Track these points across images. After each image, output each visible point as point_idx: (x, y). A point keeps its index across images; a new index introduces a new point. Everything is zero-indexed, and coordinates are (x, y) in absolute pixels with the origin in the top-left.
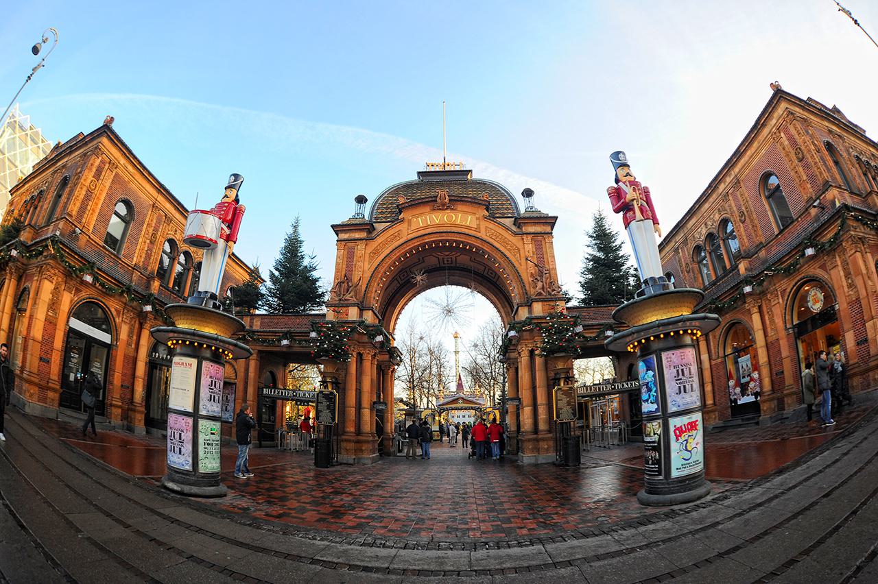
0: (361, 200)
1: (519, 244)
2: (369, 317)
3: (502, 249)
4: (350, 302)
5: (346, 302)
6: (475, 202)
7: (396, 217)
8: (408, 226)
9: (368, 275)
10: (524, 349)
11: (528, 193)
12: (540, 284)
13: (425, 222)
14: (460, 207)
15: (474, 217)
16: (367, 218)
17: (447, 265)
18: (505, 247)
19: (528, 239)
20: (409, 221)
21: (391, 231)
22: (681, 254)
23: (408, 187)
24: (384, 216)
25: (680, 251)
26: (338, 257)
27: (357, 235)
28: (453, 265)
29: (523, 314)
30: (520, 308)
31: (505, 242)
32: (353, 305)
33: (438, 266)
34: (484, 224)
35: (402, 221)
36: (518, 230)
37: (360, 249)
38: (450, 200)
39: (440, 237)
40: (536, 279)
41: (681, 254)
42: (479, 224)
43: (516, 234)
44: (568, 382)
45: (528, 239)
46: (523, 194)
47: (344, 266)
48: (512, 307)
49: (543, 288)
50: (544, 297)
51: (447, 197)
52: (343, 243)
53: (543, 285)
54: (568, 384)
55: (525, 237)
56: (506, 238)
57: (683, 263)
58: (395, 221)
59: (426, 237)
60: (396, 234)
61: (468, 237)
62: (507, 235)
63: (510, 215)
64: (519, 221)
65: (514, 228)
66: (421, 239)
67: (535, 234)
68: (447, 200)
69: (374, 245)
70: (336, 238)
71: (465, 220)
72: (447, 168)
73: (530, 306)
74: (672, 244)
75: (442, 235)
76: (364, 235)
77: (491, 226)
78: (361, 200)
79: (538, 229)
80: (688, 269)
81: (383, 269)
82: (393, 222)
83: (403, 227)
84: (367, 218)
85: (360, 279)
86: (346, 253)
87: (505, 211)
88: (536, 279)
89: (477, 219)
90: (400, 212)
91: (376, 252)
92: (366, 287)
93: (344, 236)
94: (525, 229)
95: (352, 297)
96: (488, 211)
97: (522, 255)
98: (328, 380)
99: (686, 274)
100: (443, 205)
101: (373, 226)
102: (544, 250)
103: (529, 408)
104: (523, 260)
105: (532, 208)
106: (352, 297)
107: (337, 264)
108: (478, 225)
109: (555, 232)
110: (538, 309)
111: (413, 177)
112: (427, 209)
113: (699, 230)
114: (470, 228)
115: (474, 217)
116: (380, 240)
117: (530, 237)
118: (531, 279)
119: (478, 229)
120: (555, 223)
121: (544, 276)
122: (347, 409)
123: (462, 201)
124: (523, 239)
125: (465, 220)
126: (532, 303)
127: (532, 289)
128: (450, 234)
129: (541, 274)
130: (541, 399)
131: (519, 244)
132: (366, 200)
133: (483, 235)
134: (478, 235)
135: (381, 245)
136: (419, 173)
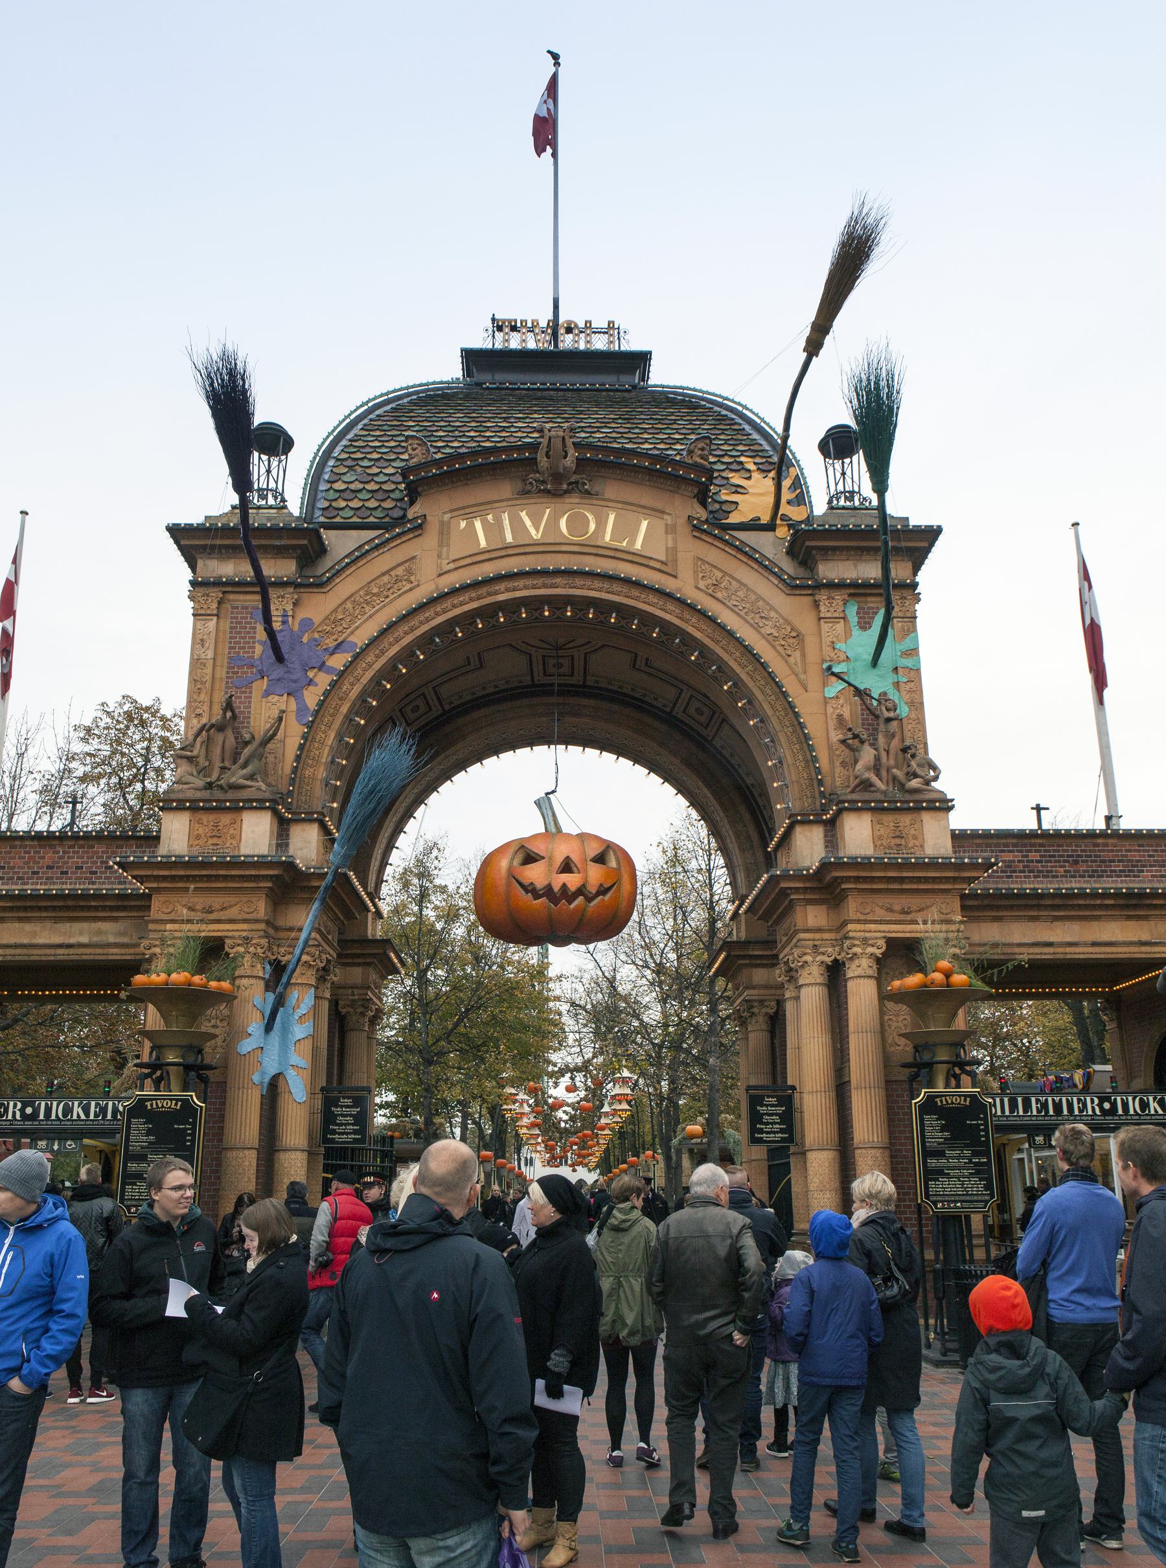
1: (805, 622)
2: (306, 846)
4: (245, 794)
5: (231, 795)
6: (660, 474)
7: (397, 513)
8: (441, 545)
10: (808, 958)
12: (867, 755)
14: (612, 489)
15: (660, 525)
16: (294, 506)
17: (556, 680)
18: (756, 628)
19: (831, 604)
20: (444, 531)
23: (430, 400)
24: (355, 504)
26: (198, 641)
28: (577, 679)
29: (808, 849)
30: (798, 829)
31: (756, 612)
32: (258, 805)
33: (527, 680)
34: (690, 549)
35: (419, 528)
36: (801, 572)
38: (580, 462)
39: (545, 586)
40: (856, 736)
42: (675, 549)
43: (793, 587)
44: (957, 1077)
46: (823, 447)
47: (221, 673)
48: (764, 827)
49: (877, 767)
50: (879, 796)
51: (573, 454)
52: (216, 593)
53: (877, 759)
54: (958, 1086)
55: (822, 596)
56: (760, 598)
58: (397, 526)
59: (502, 586)
60: (400, 571)
61: (635, 592)
64: (810, 544)
65: (788, 566)
66: (483, 591)
67: (858, 590)
68: (570, 462)
70: (188, 574)
71: (627, 532)
72: (567, 342)
73: (831, 826)
75: (549, 581)
77: (713, 555)
81: (357, 689)
82: (386, 527)
84: (294, 506)
85: (280, 719)
86: (226, 624)
88: (856, 736)
89: (670, 529)
90: (413, 493)
92: (301, 747)
94: (829, 570)
95: (251, 777)
96: (704, 504)
97: (812, 655)
98: (171, 1059)
100: (557, 477)
101: (319, 537)
103: (825, 1153)
104: (814, 677)
105: (850, 495)
106: (251, 777)
107: (196, 663)
108: (672, 552)
109: (926, 577)
111: (451, 370)
112: (506, 489)
115: (660, 525)
116: (345, 588)
117: (839, 596)
118: (836, 736)
119: (667, 568)
120: (928, 550)
121: (882, 727)
122: (231, 1155)
123: (621, 466)
124: (816, 604)
125: (627, 532)
126: (840, 812)
127: (838, 770)
128: (579, 581)
130: (867, 1124)
132: (289, 444)
133: (685, 585)
134: (670, 584)
135: (349, 605)
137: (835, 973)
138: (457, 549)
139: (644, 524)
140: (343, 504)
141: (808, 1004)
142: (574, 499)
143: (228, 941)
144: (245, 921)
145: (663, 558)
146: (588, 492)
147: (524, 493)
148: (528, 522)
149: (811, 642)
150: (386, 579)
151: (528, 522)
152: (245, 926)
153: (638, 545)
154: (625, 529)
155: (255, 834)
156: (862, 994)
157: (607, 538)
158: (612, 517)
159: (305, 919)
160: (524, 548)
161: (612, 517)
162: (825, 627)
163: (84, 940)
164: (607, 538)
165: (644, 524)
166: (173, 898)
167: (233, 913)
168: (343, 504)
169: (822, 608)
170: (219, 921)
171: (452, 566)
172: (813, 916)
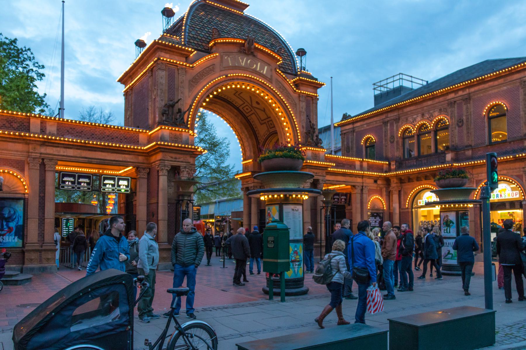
11: (302, 53)
22: (389, 127)
25: (389, 124)
41: (389, 127)
57: (389, 134)
60: (211, 67)
63: (289, 71)
74: (383, 117)
80: (392, 140)
87: (287, 67)
89: (271, 70)
99: (389, 143)
102: (311, 108)
108: (271, 76)
113: (415, 116)
139: (266, 67)
140: (192, 41)
142: (251, 57)
143: (181, 167)
144: (186, 162)
145: (269, 77)
146: (254, 56)
147: (240, 52)
148: (241, 61)
149: (298, 106)
150: (208, 69)
151: (241, 61)
152: (185, 164)
153: (265, 72)
154: (262, 68)
157: (258, 69)
158: (259, 64)
161: (259, 64)
162: (301, 103)
163: (121, 159)
164: (258, 69)
165: (266, 67)
166: (167, 154)
167: (181, 160)
168: (192, 41)
169: (301, 98)
170: (178, 162)
171: (223, 69)
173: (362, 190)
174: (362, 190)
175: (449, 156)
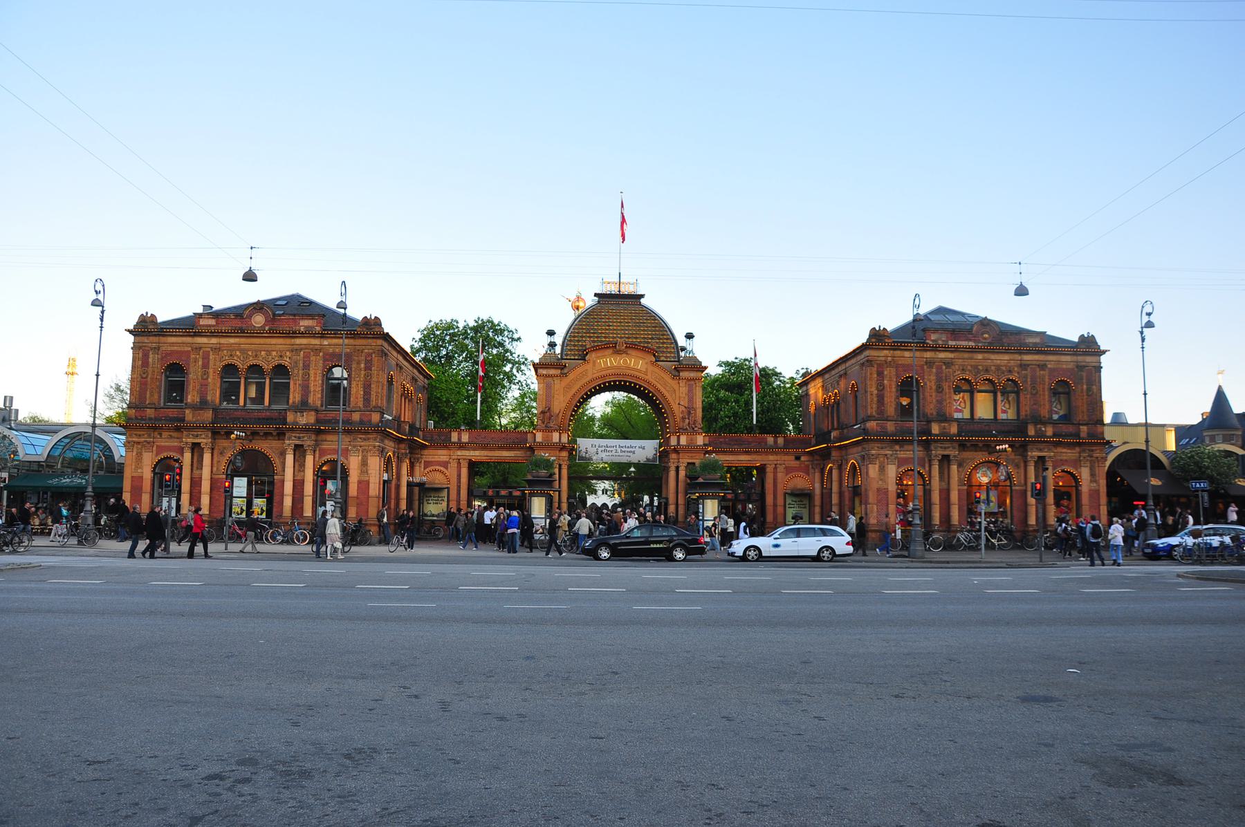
0: (551, 333)
1: (676, 387)
3: (662, 390)
9: (564, 405)
11: (689, 336)
13: (607, 363)
21: (579, 370)
27: (552, 372)
34: (651, 368)
37: (558, 385)
45: (682, 383)
62: (667, 378)
67: (689, 380)
69: (566, 381)
76: (558, 372)
77: (656, 370)
78: (551, 333)
79: (693, 375)
83: (589, 367)
91: (569, 387)
93: (540, 371)
94: (684, 374)
110: (684, 440)
114: (639, 371)
116: (571, 376)
129: (689, 413)
130: (681, 501)
131: (676, 387)
133: (649, 377)
136: (596, 295)
137: (677, 468)
138: (597, 367)
141: (672, 473)
155: (555, 437)
156: (682, 473)
159: (565, 454)
160: (612, 368)
172: (674, 456)
173: (776, 468)
174: (776, 468)
175: (834, 434)
